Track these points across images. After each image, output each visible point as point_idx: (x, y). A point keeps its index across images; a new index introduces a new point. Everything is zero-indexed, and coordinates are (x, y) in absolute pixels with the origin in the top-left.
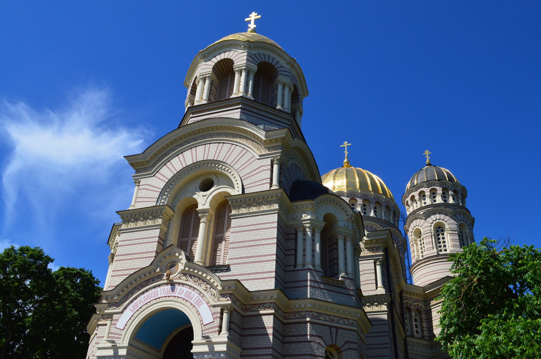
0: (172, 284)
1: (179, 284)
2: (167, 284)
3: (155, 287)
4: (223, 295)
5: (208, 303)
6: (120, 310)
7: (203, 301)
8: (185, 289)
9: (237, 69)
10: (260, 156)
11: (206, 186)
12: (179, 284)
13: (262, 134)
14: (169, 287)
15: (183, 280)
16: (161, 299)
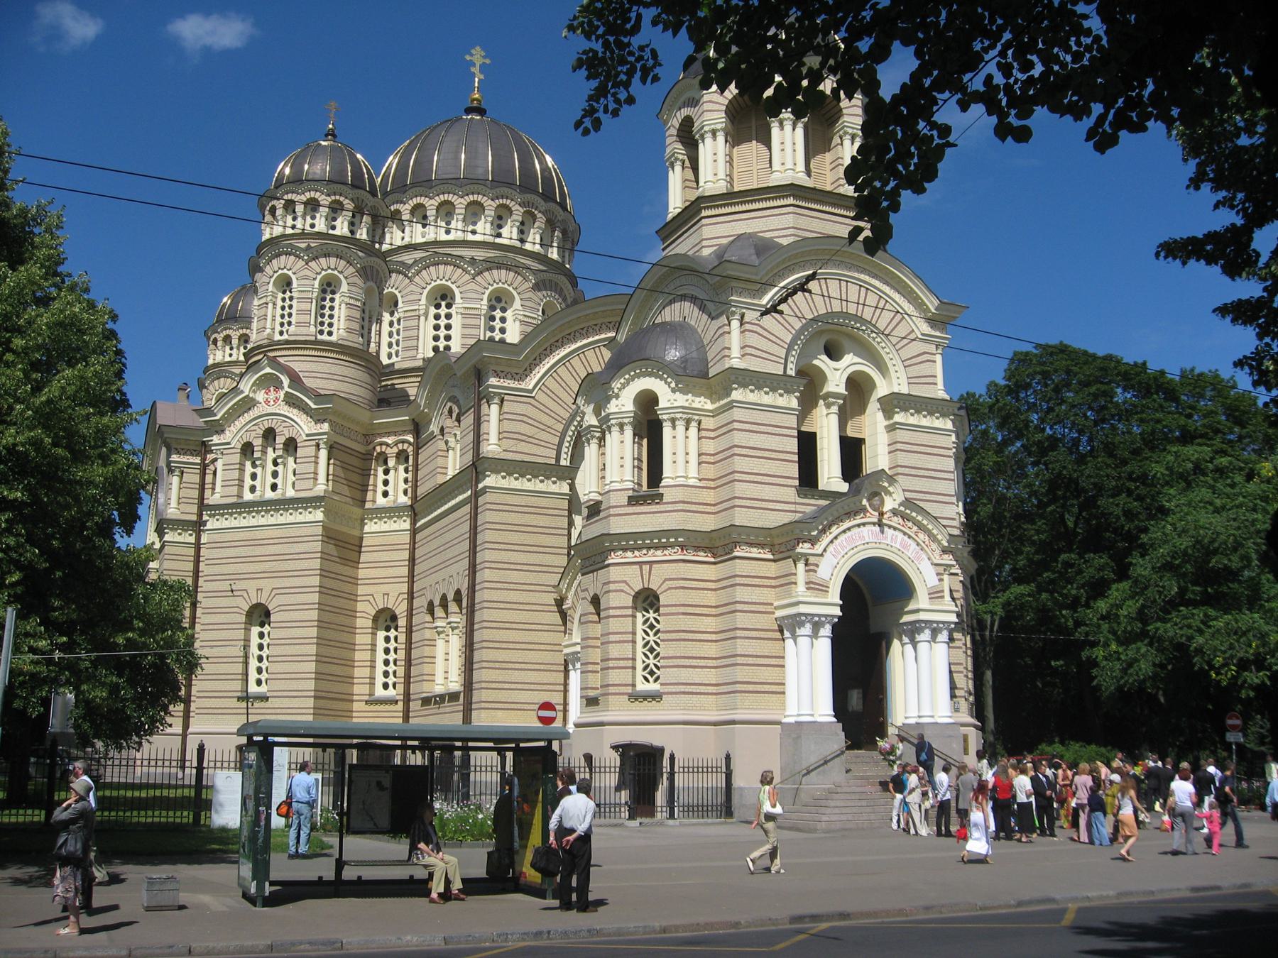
0: (880, 524)
1: (890, 527)
2: (874, 524)
3: (859, 526)
4: (945, 551)
5: (929, 559)
6: (820, 552)
7: (924, 556)
8: (900, 535)
9: (850, 131)
10: (923, 334)
11: (833, 352)
12: (890, 527)
13: (931, 302)
14: (877, 528)
15: (896, 521)
16: (870, 545)
